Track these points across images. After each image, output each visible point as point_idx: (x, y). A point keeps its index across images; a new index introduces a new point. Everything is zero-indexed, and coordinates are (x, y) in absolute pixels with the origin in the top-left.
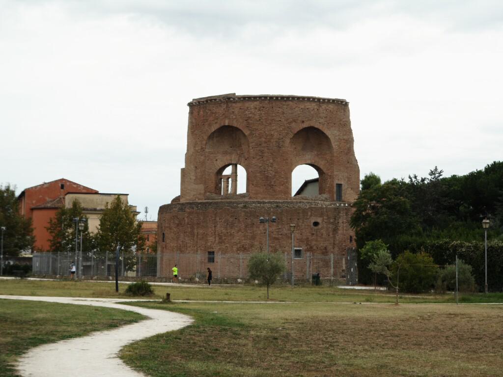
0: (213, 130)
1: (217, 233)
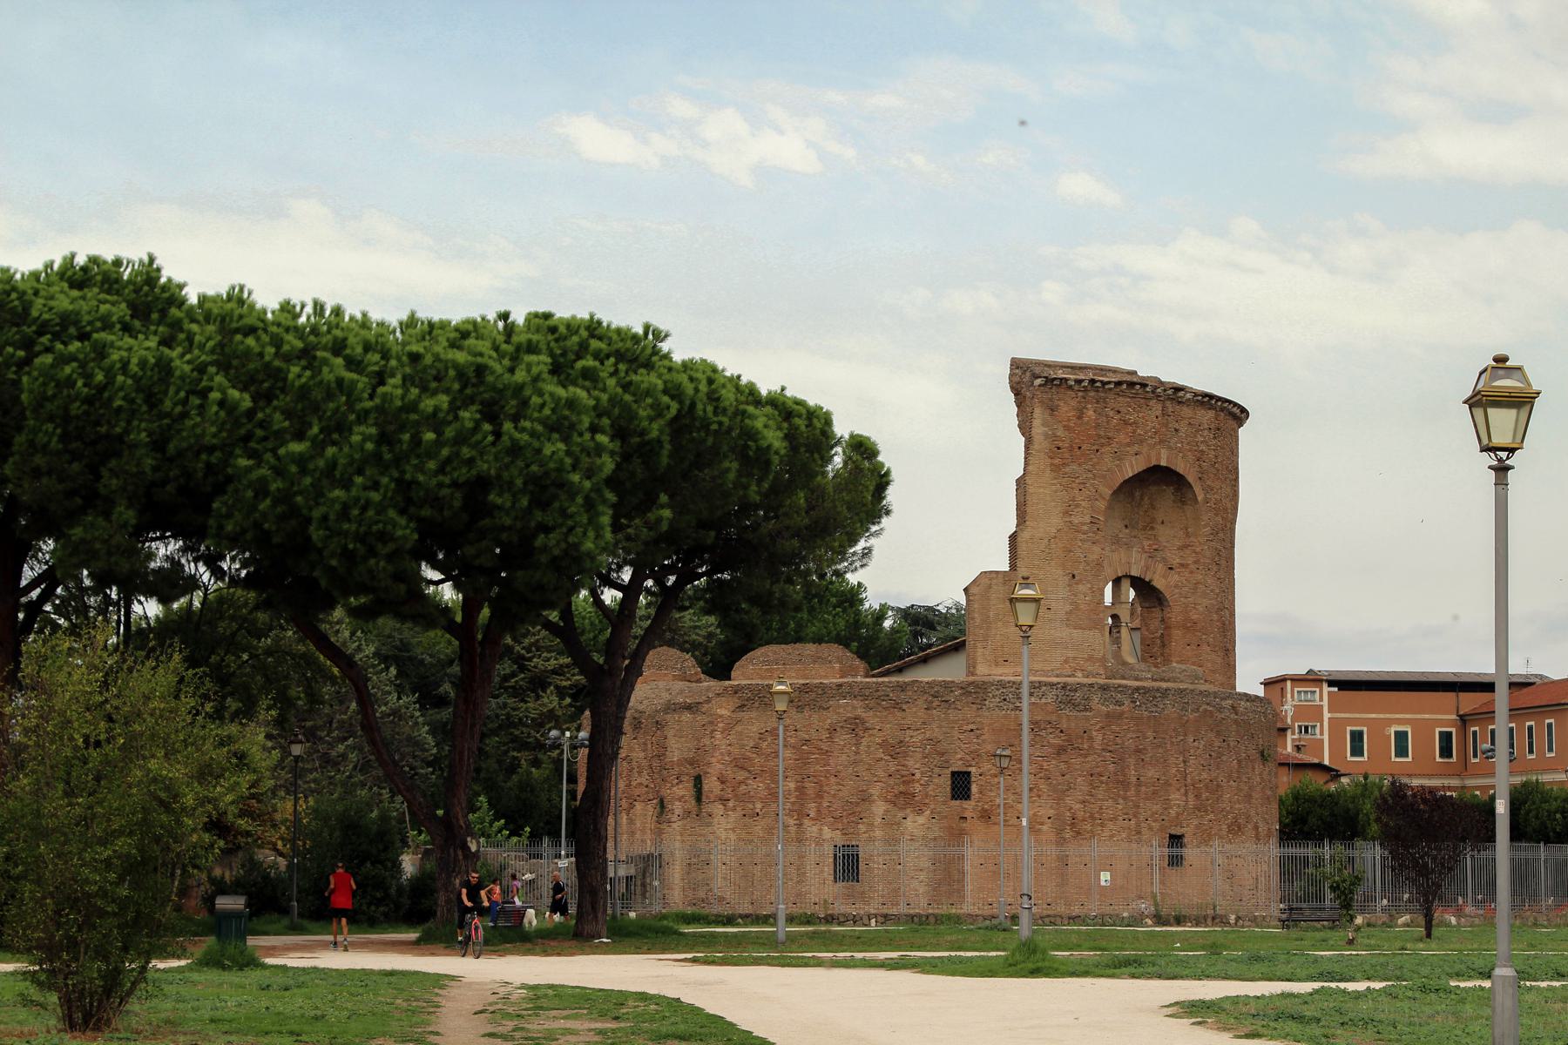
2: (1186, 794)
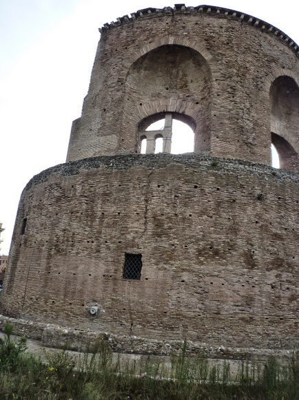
0: (145, 52)
1: (149, 214)
2: (145, 223)
